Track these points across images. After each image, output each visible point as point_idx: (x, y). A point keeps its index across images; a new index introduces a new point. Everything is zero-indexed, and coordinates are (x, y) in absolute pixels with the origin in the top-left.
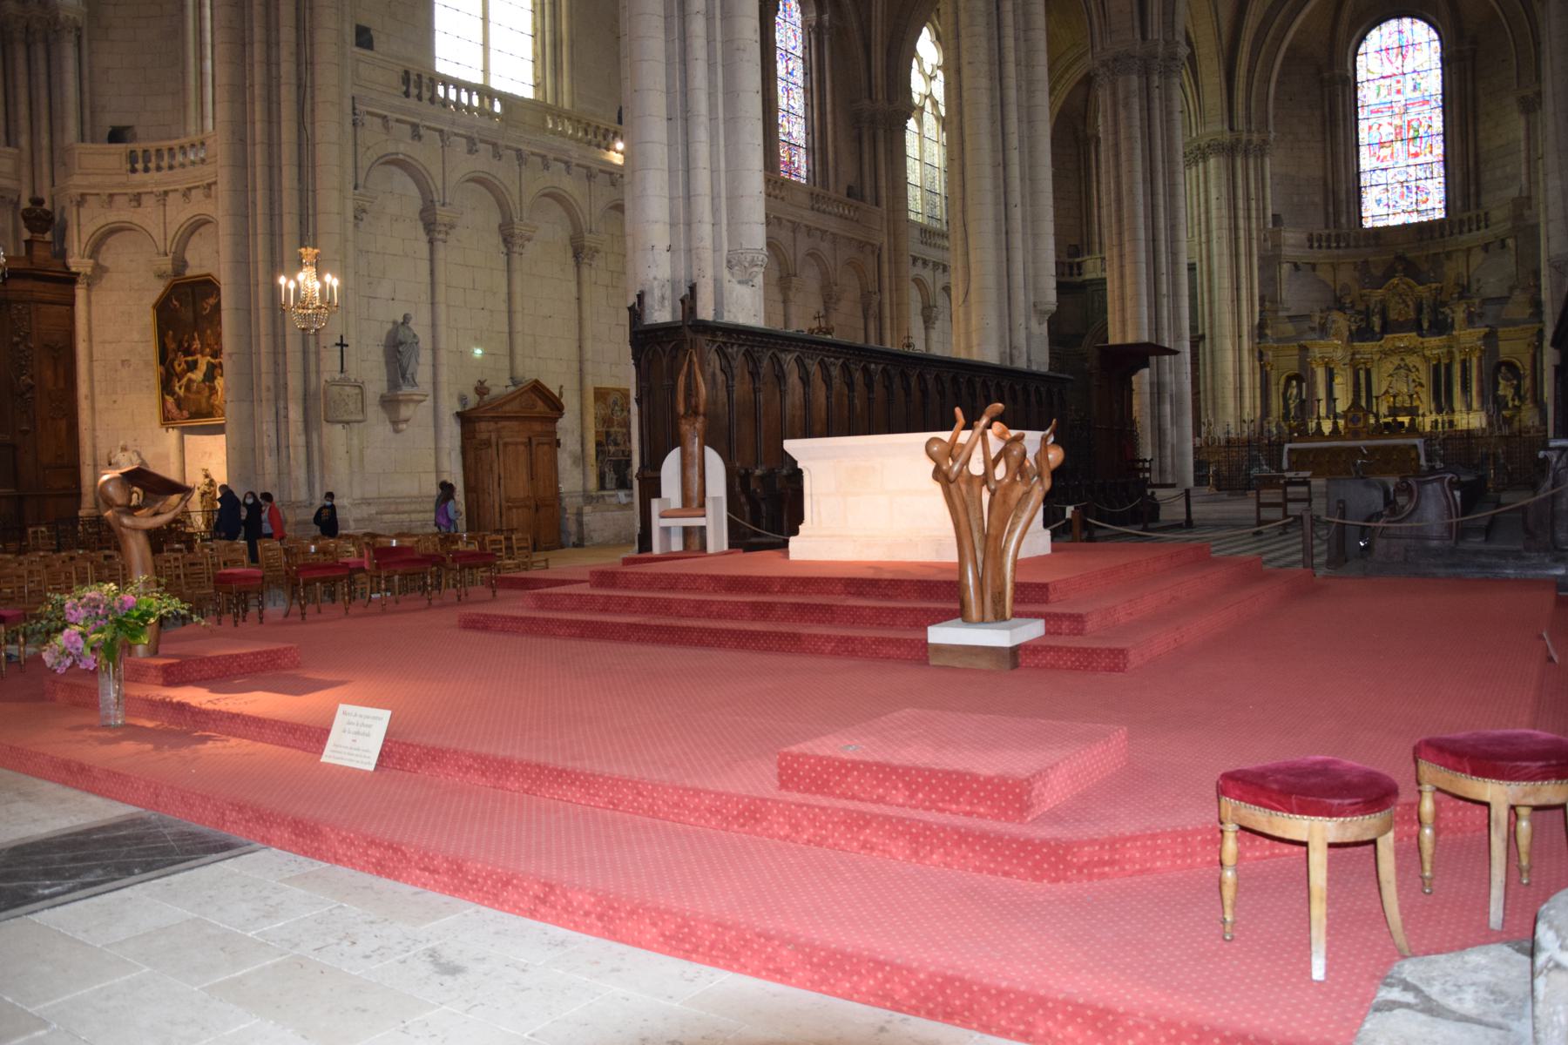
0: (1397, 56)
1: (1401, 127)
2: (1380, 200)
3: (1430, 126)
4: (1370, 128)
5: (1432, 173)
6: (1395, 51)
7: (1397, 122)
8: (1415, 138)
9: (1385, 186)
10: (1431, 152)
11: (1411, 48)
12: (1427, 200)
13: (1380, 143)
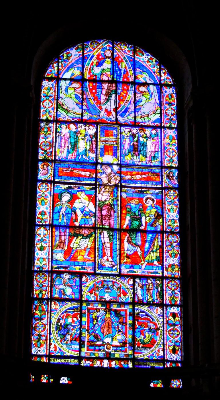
0: (109, 94)
1: (111, 207)
2: (66, 327)
3: (159, 216)
4: (56, 198)
5: (162, 295)
6: (105, 86)
7: (103, 196)
8: (131, 231)
9: (76, 305)
10: (160, 260)
11: (131, 89)
12: (153, 342)
13: (71, 227)
